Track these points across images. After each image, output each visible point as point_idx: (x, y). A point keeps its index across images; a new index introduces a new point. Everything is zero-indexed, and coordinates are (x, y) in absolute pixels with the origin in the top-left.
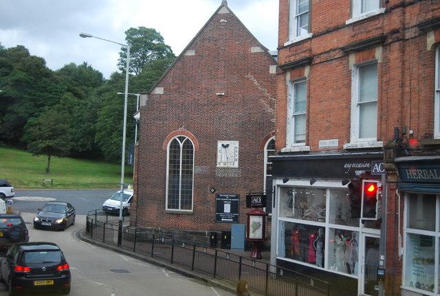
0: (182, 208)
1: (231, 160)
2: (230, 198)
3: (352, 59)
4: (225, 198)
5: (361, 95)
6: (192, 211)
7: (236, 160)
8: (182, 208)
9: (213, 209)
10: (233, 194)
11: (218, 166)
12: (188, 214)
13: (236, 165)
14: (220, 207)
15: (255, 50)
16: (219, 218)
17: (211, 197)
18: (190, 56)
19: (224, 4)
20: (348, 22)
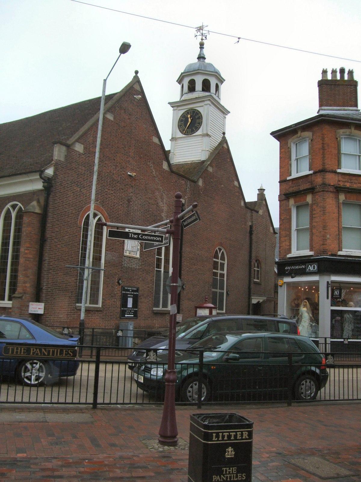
0: (90, 304)
1: (135, 249)
2: (133, 291)
3: (292, 201)
4: (128, 290)
5: (297, 226)
6: (100, 305)
7: (138, 250)
8: (90, 304)
9: (119, 303)
10: (135, 287)
11: (125, 254)
12: (98, 310)
13: (138, 256)
14: (124, 303)
15: (156, 140)
16: (123, 313)
17: (117, 290)
18: (110, 120)
19: (136, 80)
20: (288, 178)
